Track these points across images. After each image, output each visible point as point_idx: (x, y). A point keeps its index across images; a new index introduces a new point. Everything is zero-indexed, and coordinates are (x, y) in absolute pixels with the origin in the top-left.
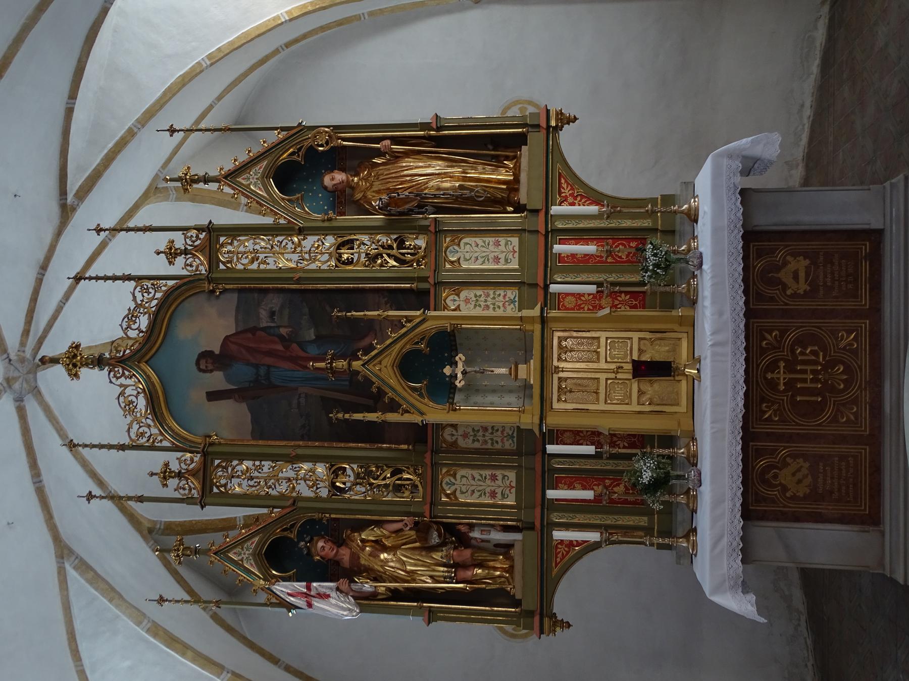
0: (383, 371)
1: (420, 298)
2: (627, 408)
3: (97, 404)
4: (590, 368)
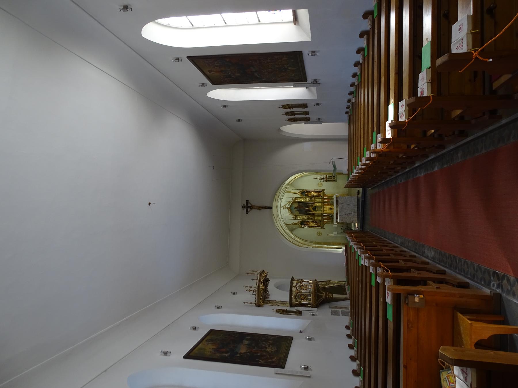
0: (311, 209)
1: (313, 203)
2: (329, 212)
3: (286, 212)
4: (327, 209)
